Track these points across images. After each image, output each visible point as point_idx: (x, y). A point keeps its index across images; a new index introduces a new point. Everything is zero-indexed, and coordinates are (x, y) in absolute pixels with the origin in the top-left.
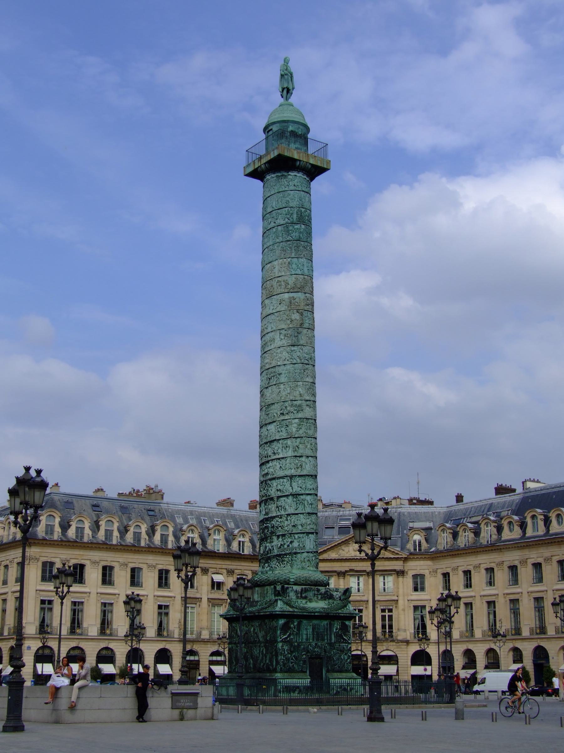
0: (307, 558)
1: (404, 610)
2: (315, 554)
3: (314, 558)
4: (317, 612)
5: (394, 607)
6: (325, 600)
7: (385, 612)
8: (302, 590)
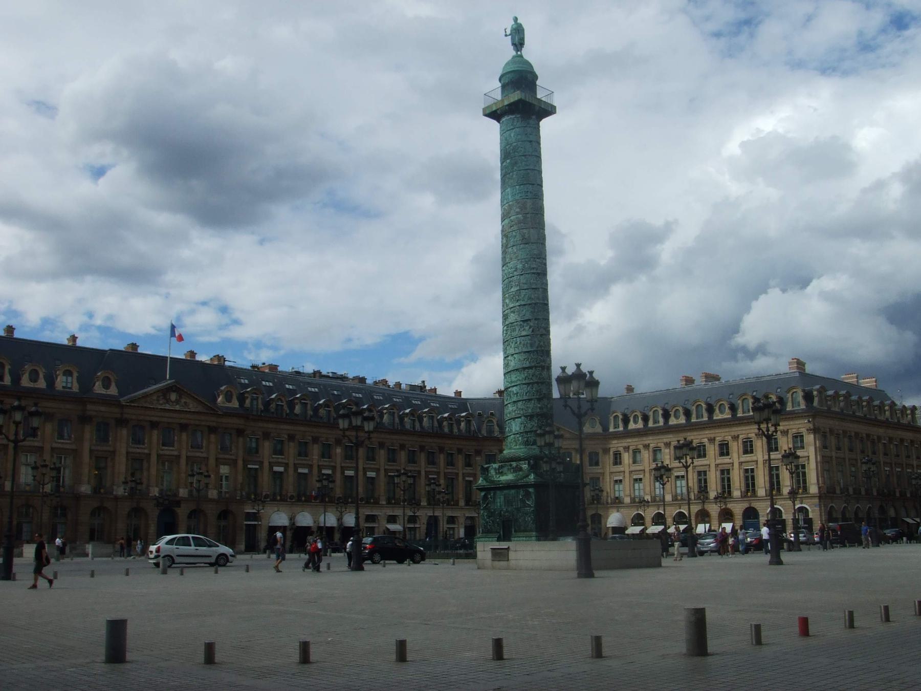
0: (513, 440)
2: (522, 434)
3: (520, 438)
4: (502, 484)
6: (517, 472)
8: (499, 467)
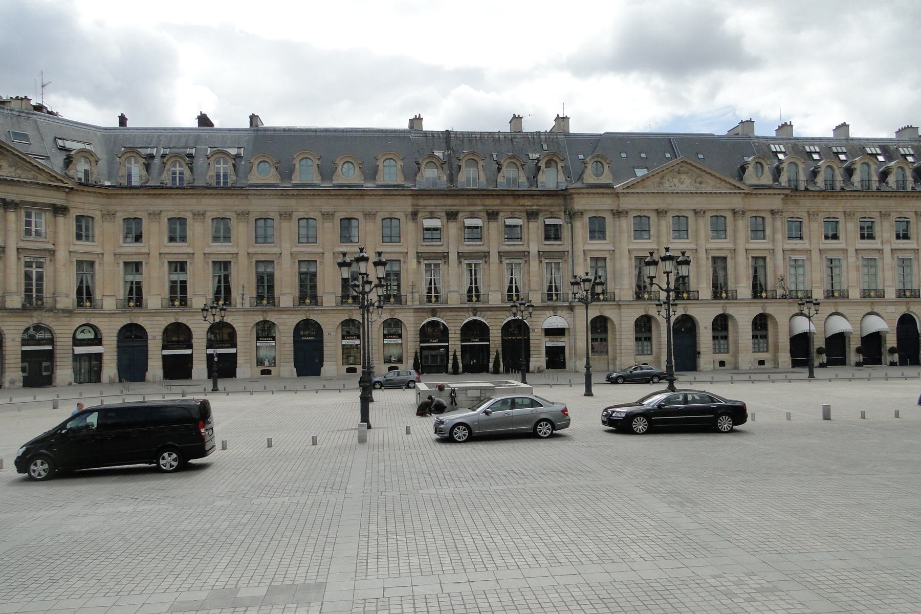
1: (65, 265)
5: (48, 259)
7: (31, 267)
